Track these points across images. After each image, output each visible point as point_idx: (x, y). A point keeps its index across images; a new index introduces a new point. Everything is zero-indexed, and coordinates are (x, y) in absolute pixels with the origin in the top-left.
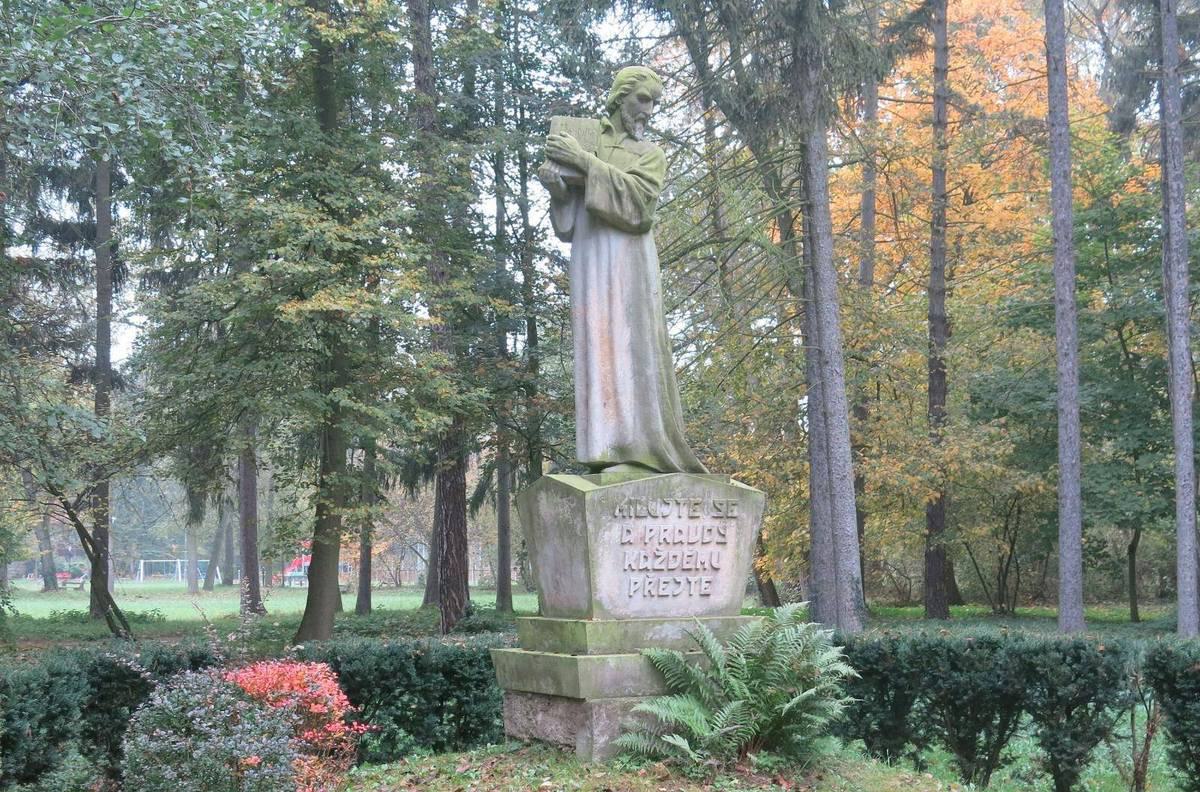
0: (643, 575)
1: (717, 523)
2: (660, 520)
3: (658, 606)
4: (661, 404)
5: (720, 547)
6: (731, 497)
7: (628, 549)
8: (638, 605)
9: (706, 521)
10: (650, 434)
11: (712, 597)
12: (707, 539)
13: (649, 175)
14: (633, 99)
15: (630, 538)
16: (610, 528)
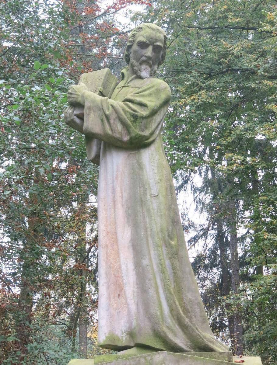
4: (166, 288)
10: (151, 318)
13: (138, 99)
14: (135, 47)
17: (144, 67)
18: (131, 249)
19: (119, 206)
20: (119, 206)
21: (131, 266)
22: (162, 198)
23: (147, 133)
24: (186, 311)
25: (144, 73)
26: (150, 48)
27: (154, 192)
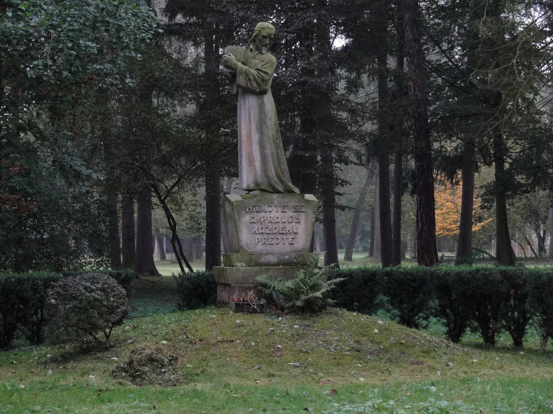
1: (295, 214)
2: (268, 213)
3: (269, 248)
4: (274, 164)
5: (297, 225)
6: (301, 203)
7: (254, 225)
8: (260, 247)
10: (267, 177)
11: (295, 245)
12: (291, 221)
13: (265, 70)
14: (260, 37)
15: (255, 220)
16: (245, 216)
17: (263, 48)
18: (258, 145)
20: (253, 123)
24: (282, 174)
26: (268, 39)
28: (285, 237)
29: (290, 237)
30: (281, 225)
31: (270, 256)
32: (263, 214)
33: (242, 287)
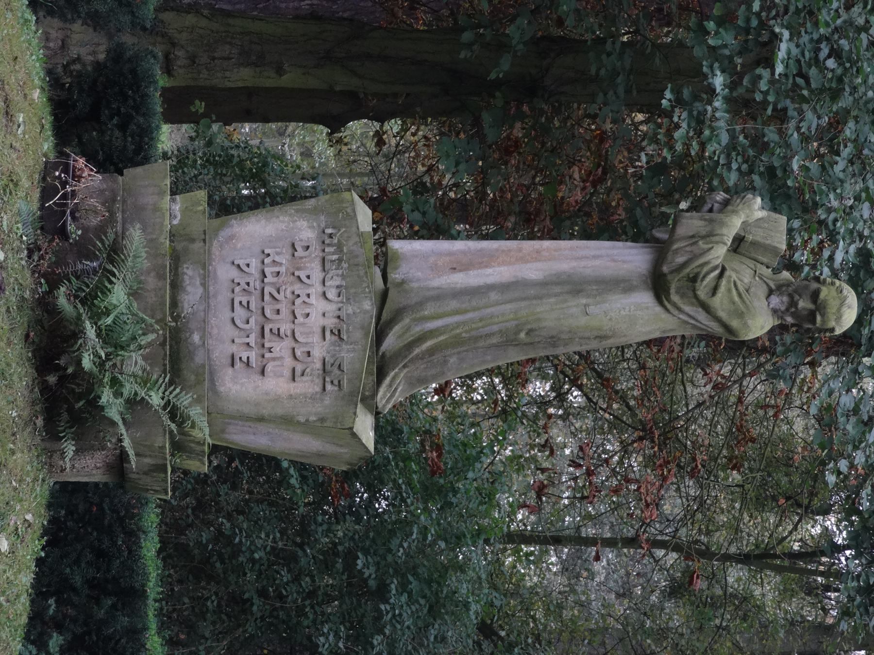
0: (257, 275)
1: (319, 365)
2: (320, 289)
3: (223, 297)
5: (287, 373)
6: (349, 380)
7: (287, 251)
8: (224, 273)
9: (318, 352)
10: (421, 304)
11: (230, 371)
12: (298, 353)
15: (300, 252)
16: (311, 227)
17: (785, 299)
18: (514, 280)
19: (574, 264)
20: (574, 264)
21: (490, 280)
22: (583, 321)
23: (675, 298)
24: (431, 351)
25: (775, 300)
26: (811, 306)
27: (592, 309)
28: (252, 340)
29: (253, 355)
30: (286, 328)
31: (200, 290)
32: (317, 274)
33: (114, 200)
